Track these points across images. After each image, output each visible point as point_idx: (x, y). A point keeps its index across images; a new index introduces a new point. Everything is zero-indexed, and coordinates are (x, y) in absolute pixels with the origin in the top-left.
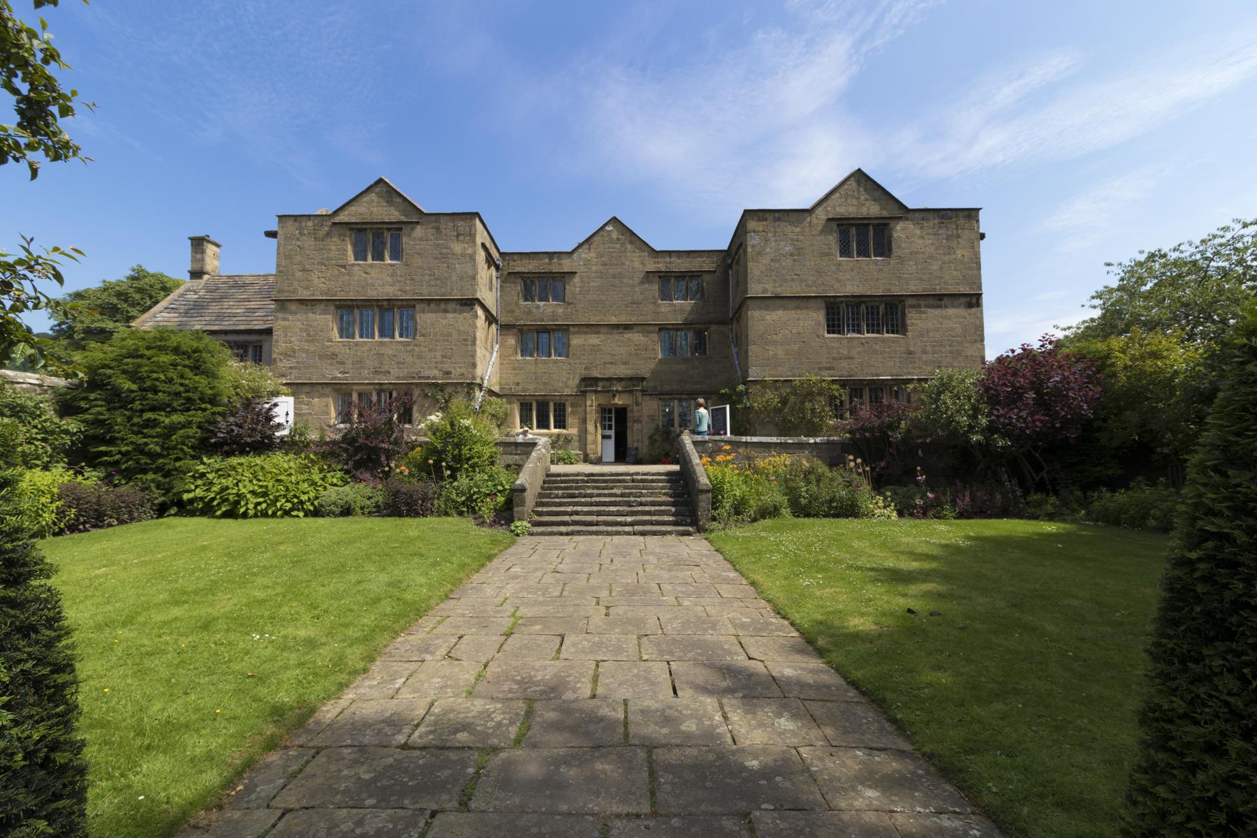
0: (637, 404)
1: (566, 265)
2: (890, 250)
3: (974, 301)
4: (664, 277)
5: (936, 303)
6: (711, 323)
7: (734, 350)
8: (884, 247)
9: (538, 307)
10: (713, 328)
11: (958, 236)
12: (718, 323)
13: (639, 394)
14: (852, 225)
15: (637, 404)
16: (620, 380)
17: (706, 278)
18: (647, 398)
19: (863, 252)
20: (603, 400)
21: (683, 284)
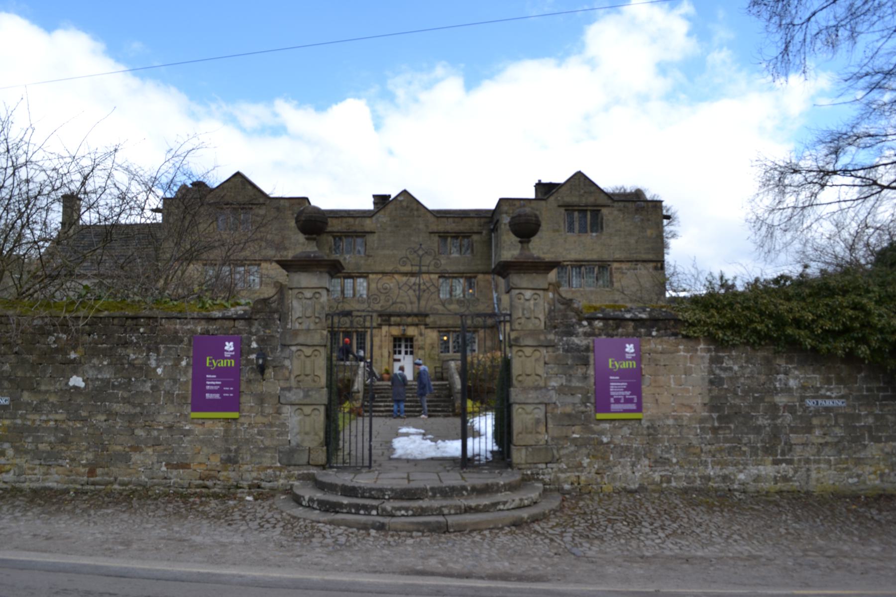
0: (421, 334)
1: (369, 224)
2: (602, 228)
3: (659, 265)
4: (443, 236)
5: (633, 266)
6: (478, 273)
7: (495, 295)
8: (597, 225)
9: (345, 259)
10: (480, 276)
11: (648, 220)
12: (484, 273)
13: (422, 327)
14: (575, 210)
15: (421, 334)
16: (409, 315)
17: (475, 237)
18: (429, 330)
19: (583, 230)
20: (396, 331)
21: (457, 242)
